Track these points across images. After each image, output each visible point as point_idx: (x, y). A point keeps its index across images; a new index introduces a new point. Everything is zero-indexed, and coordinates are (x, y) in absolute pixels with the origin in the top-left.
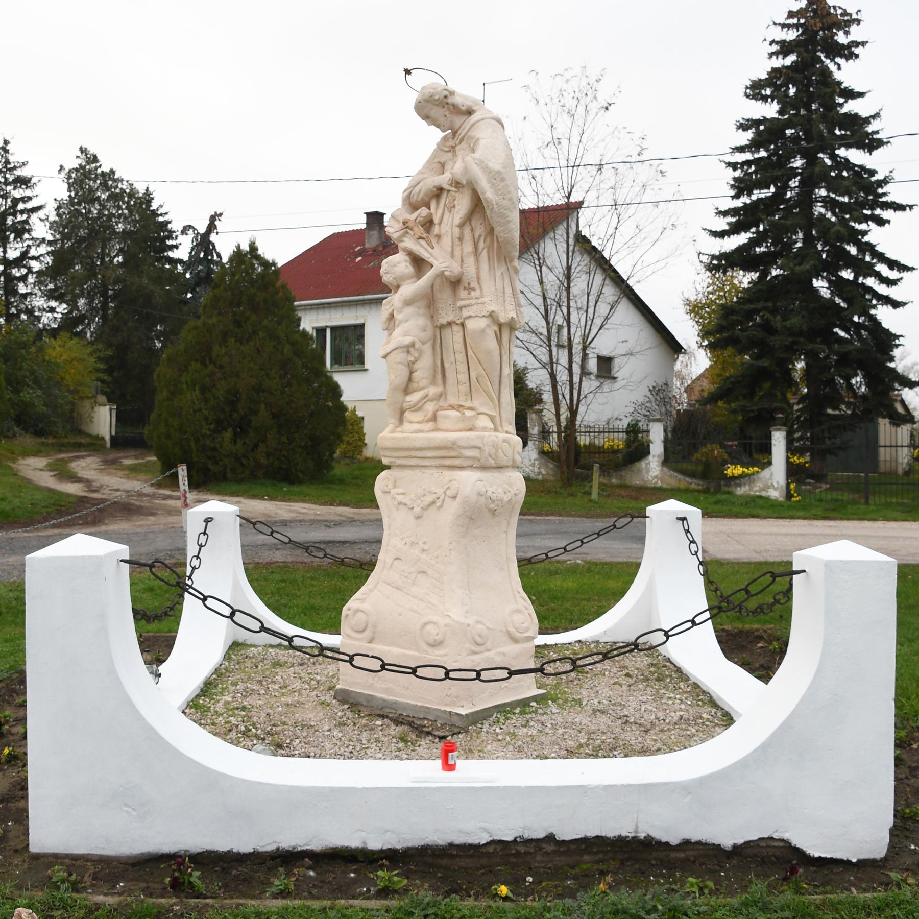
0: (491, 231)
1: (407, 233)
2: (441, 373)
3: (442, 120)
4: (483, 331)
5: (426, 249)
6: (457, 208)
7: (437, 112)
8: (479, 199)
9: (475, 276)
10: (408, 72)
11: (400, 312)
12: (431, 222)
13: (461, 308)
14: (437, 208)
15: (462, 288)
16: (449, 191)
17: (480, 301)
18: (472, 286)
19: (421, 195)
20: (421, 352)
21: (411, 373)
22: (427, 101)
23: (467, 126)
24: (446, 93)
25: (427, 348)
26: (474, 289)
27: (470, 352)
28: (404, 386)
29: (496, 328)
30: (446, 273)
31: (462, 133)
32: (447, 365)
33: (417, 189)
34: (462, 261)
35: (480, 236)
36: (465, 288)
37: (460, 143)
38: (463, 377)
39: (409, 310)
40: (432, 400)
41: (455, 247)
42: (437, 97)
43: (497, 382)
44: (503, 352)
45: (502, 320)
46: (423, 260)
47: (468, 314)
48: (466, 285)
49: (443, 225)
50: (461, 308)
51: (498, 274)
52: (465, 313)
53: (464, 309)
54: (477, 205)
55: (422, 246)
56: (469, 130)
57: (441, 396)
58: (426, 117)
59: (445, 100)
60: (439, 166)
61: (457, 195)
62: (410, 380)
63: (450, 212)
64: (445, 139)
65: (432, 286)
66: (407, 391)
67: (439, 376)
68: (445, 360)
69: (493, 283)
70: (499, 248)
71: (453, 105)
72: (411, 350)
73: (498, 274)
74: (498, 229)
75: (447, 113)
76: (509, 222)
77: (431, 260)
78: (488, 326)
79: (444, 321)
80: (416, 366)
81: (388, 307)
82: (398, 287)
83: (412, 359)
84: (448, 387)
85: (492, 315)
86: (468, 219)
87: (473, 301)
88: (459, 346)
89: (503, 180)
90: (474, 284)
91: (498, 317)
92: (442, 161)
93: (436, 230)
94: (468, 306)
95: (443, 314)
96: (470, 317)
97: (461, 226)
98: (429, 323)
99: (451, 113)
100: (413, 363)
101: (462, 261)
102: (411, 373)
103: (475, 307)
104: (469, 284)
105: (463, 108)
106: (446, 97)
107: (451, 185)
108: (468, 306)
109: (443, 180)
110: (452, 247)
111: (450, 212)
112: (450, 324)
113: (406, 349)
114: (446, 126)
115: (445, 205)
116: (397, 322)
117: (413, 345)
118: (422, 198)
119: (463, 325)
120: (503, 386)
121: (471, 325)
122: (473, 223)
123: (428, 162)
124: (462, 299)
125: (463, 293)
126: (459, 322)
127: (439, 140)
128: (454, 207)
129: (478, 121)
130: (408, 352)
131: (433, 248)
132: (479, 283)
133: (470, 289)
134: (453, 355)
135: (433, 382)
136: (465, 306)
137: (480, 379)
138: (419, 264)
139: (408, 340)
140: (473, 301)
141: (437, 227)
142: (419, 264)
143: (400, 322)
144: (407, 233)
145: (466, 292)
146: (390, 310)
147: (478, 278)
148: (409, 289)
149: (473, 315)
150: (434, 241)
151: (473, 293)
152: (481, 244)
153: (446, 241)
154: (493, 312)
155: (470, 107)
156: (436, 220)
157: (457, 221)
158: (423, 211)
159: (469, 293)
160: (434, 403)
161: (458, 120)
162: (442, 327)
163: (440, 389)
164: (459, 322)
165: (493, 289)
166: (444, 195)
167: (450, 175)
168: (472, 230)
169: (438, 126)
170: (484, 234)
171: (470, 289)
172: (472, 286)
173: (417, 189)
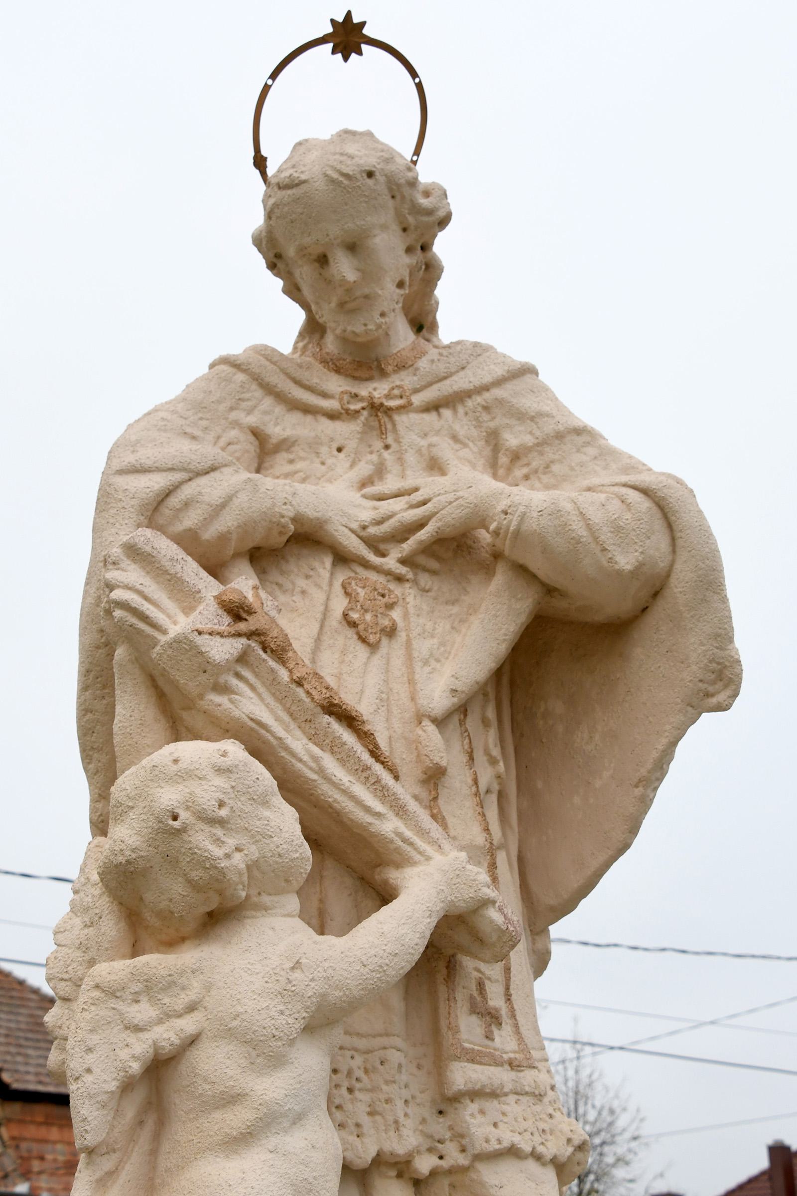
17: (528, 1077)
19: (227, 522)
37: (434, 407)
48: (475, 994)
55: (334, 747)
77: (389, 826)
81: (143, 1012)
96: (513, 1152)
103: (512, 1107)
104: (481, 986)
118: (223, 538)
124: (474, 1058)
125: (468, 1029)
126: (424, 1164)
136: (475, 1094)
173: (211, 489)
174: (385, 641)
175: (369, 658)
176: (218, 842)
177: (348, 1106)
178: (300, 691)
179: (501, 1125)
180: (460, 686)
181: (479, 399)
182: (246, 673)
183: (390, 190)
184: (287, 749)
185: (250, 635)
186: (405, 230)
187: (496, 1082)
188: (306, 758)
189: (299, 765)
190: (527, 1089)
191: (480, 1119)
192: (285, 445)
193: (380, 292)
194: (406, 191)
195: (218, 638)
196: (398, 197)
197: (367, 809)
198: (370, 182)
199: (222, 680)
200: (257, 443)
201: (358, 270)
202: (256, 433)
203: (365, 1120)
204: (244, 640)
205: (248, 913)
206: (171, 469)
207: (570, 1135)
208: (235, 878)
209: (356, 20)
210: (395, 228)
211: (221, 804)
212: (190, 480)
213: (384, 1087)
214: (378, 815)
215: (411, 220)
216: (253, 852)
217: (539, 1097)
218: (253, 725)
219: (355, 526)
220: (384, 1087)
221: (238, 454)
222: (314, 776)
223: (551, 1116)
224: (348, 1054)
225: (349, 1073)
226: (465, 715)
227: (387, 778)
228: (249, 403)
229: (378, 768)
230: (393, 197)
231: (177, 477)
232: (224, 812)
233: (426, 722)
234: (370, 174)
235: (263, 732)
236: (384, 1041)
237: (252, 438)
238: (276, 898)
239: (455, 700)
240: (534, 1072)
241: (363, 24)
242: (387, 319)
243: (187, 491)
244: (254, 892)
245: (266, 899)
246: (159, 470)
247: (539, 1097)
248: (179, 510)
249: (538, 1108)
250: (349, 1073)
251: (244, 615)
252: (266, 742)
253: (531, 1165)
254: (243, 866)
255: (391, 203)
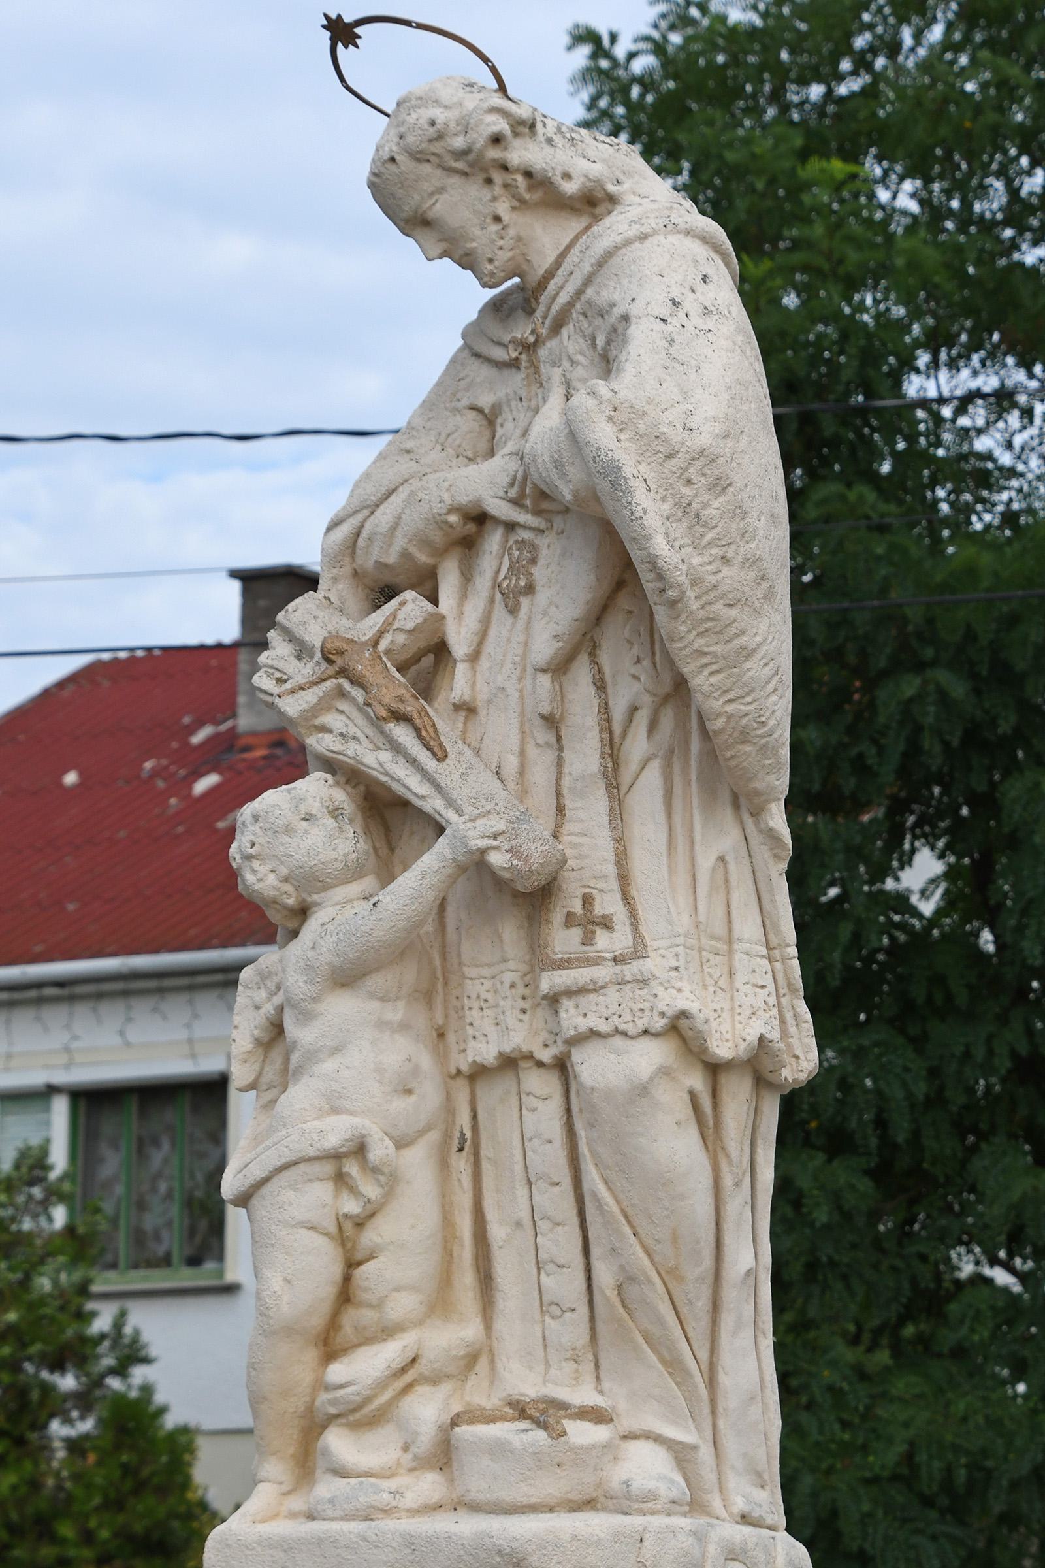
0: (679, 690)
1: (342, 694)
2: (473, 1264)
3: (482, 238)
4: (642, 1091)
5: (413, 762)
6: (543, 596)
7: (460, 203)
8: (628, 564)
9: (611, 869)
10: (342, 32)
11: (306, 1017)
12: (440, 650)
13: (553, 1000)
14: (463, 596)
15: (558, 917)
16: (511, 526)
17: (631, 970)
18: (598, 910)
19: (400, 542)
20: (391, 1181)
21: (351, 1264)
22: (419, 157)
23: (580, 263)
24: (501, 125)
25: (417, 1164)
26: (606, 923)
27: (592, 1177)
28: (318, 1321)
29: (697, 1081)
30: (497, 859)
31: (561, 292)
32: (497, 1232)
33: (383, 518)
34: (560, 810)
35: (633, 709)
36: (570, 920)
37: (557, 327)
38: (566, 1285)
39: (343, 1009)
40: (434, 1380)
41: (532, 752)
42: (459, 142)
43: (703, 1304)
44: (728, 1181)
45: (722, 1050)
46: (404, 804)
47: (583, 1024)
48: (577, 907)
49: (484, 663)
50: (553, 1000)
51: (706, 862)
52: (573, 1018)
53: (567, 1004)
54: (619, 585)
55: (397, 748)
56: (588, 281)
57: (471, 1360)
58: (415, 224)
59: (493, 153)
60: (469, 423)
61: (542, 542)
62: (345, 1295)
63: (513, 611)
64: (497, 309)
65: (442, 906)
66: (330, 1346)
67: (466, 1279)
68: (491, 1215)
69: (684, 901)
70: (711, 756)
71: (528, 174)
72: (352, 1168)
73: (706, 862)
74: (701, 682)
75: (503, 208)
76: (747, 653)
77: (433, 804)
78: (664, 1072)
79: (486, 1051)
80: (370, 1237)
82: (303, 912)
83: (352, 1206)
84: (499, 1325)
85: (679, 1030)
86: (584, 642)
87: (603, 973)
88: (550, 1156)
89: (720, 485)
90: (609, 904)
91: (701, 1038)
92: (486, 400)
93: (460, 683)
94: (582, 991)
95: (481, 1020)
96: (593, 1034)
97: (560, 667)
98: (426, 1061)
99: (521, 204)
100: (360, 1223)
101: (560, 810)
102: (351, 1264)
103: (612, 995)
104: (587, 900)
105: (570, 188)
106: (497, 140)
107: (517, 502)
108: (582, 991)
109: (484, 482)
110: (522, 753)
111: (513, 611)
112: (510, 1063)
113: (328, 1168)
114: (502, 257)
115: (496, 585)
116: (295, 1058)
117: (360, 1149)
118: (405, 555)
119: (562, 1066)
120: (727, 1321)
121: (596, 1067)
122: (604, 659)
123: (429, 406)
124: (559, 965)
125: (563, 940)
126: (545, 1056)
127: (474, 316)
128: (530, 589)
129: (628, 242)
130: (341, 1179)
131: (441, 756)
132: (627, 898)
133: (591, 923)
134: (522, 1192)
135: (440, 1303)
136: (570, 993)
137: (633, 1291)
138: (389, 819)
139: (334, 1132)
140: (603, 973)
141: (461, 669)
142: (389, 819)
143: (312, 1056)
144: (342, 694)
145: (576, 934)
146: (269, 1009)
147: (624, 879)
148: (346, 918)
149: (603, 1027)
150: (447, 727)
151: (602, 940)
152: (637, 746)
153: (502, 731)
154: (684, 1014)
155: (599, 183)
156: (459, 645)
157: (544, 648)
158: (410, 608)
159: (588, 940)
160: (446, 1388)
161: (547, 237)
162: (478, 1074)
163: (470, 1330)
164: (545, 1056)
165: (685, 921)
166: (494, 541)
167: (514, 465)
168: (600, 685)
169: (467, 261)
170: (647, 699)
171: (591, 923)
172: (598, 910)
173: (383, 518)
174: (525, 602)
175: (513, 624)
176: (254, 871)
177: (477, 1023)
178: (369, 709)
179: (589, 1014)
180: (560, 630)
181: (578, 306)
182: (343, 705)
183: (419, 160)
184: (362, 764)
185: (336, 676)
186: (466, 174)
187: (581, 983)
188: (377, 766)
189: (374, 773)
190: (627, 978)
191: (572, 1011)
192: (496, 410)
193: (474, 244)
194: (436, 148)
195: (302, 693)
196: (432, 158)
197: (414, 794)
198: (392, 167)
199: (317, 722)
200: (480, 416)
201: (441, 240)
202: (474, 408)
203: (491, 1031)
204: (329, 684)
205: (315, 909)
206: (356, 512)
207: (665, 1009)
208: (272, 893)
209: (334, 16)
210: (454, 181)
211: (253, 845)
212: (372, 513)
213: (502, 1003)
214: (423, 797)
215: (460, 165)
216: (284, 871)
217: (644, 982)
218: (331, 754)
219: (501, 494)
220: (502, 1003)
221: (458, 442)
222: (383, 778)
223: (656, 995)
224: (477, 982)
225: (478, 997)
226: (594, 647)
227: (429, 763)
228: (468, 380)
229: (424, 757)
230: (429, 161)
231: (359, 517)
232: (251, 851)
233: (539, 675)
234: (393, 160)
235: (340, 757)
236: (503, 966)
237: (474, 413)
238: (322, 895)
239: (561, 644)
240: (641, 961)
241: (339, 16)
242: (496, 263)
243: (368, 525)
244: (304, 895)
245: (316, 897)
246: (350, 516)
247: (644, 982)
248: (368, 546)
249: (641, 992)
250: (478, 997)
251: (333, 657)
252: (347, 763)
253: (618, 1041)
254: (276, 883)
255: (427, 169)
